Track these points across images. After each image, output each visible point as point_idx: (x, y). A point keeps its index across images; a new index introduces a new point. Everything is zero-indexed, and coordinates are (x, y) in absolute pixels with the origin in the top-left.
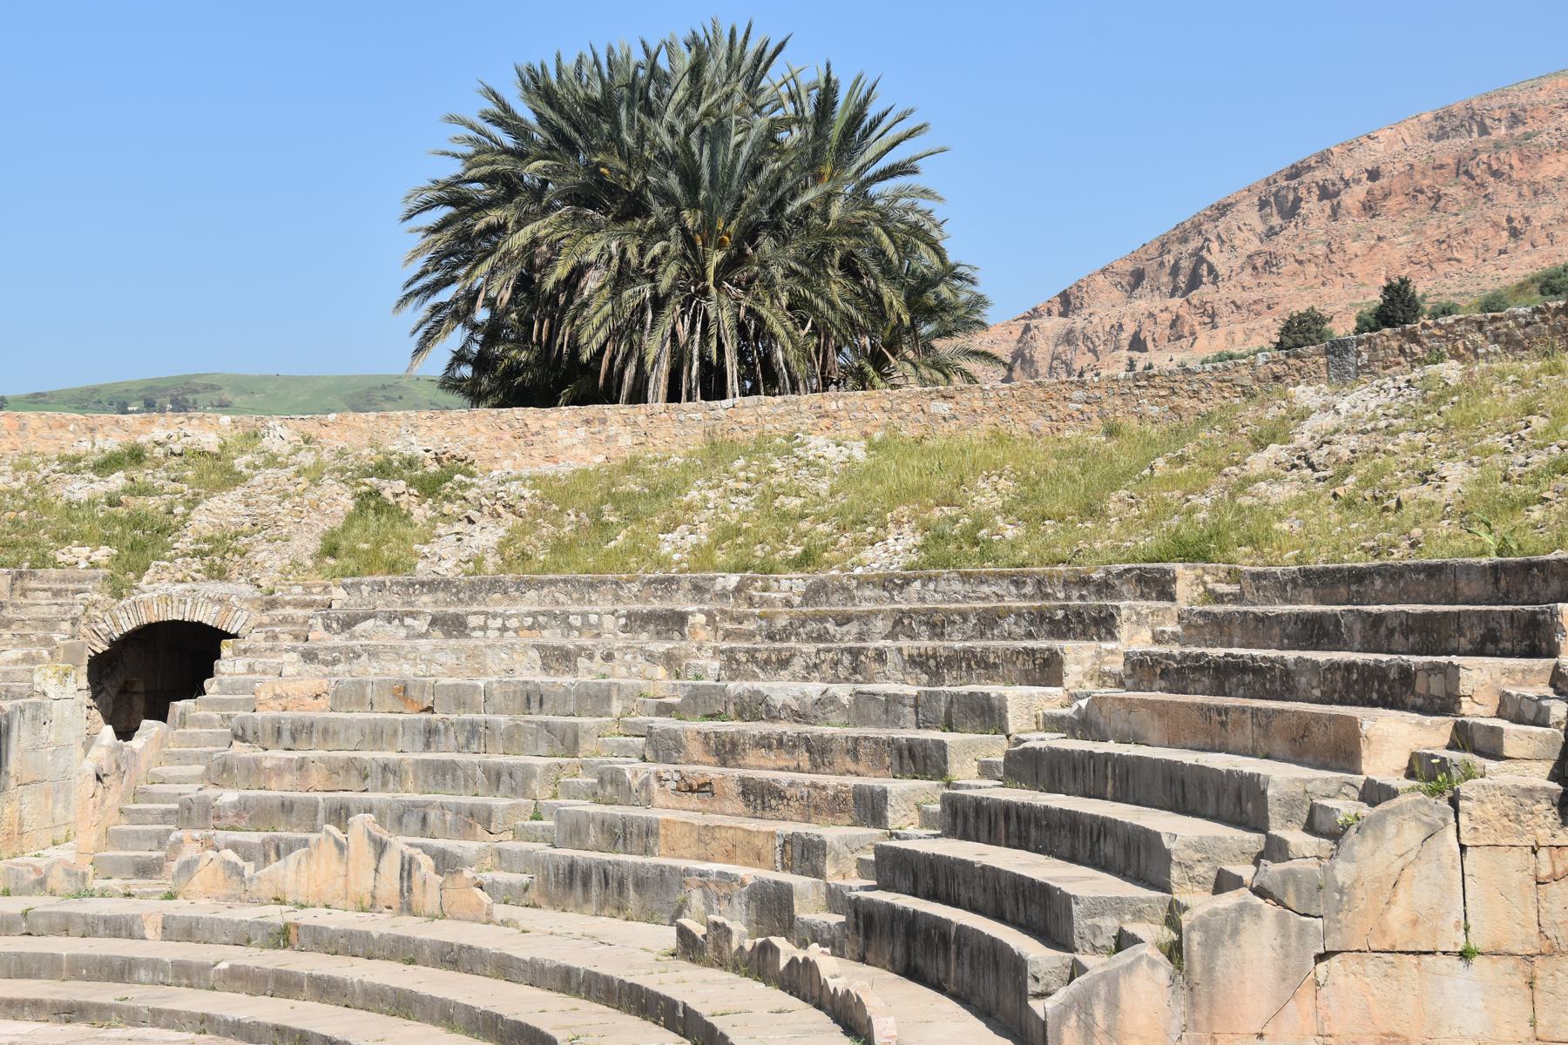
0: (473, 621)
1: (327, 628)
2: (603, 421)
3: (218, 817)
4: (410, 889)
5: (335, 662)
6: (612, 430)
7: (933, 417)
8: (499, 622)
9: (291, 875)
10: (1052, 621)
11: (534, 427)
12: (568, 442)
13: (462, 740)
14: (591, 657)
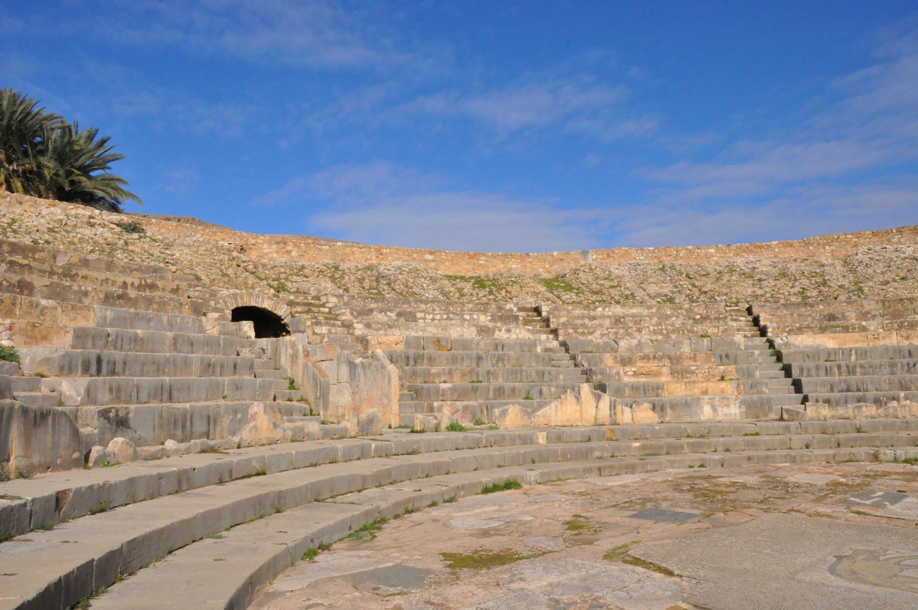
0: (419, 315)
1: (352, 314)
2: (286, 243)
4: (615, 414)
5: (380, 329)
6: (289, 248)
7: (426, 261)
8: (431, 316)
9: (553, 413)
10: (694, 319)
11: (253, 241)
13: (494, 362)
14: (500, 330)
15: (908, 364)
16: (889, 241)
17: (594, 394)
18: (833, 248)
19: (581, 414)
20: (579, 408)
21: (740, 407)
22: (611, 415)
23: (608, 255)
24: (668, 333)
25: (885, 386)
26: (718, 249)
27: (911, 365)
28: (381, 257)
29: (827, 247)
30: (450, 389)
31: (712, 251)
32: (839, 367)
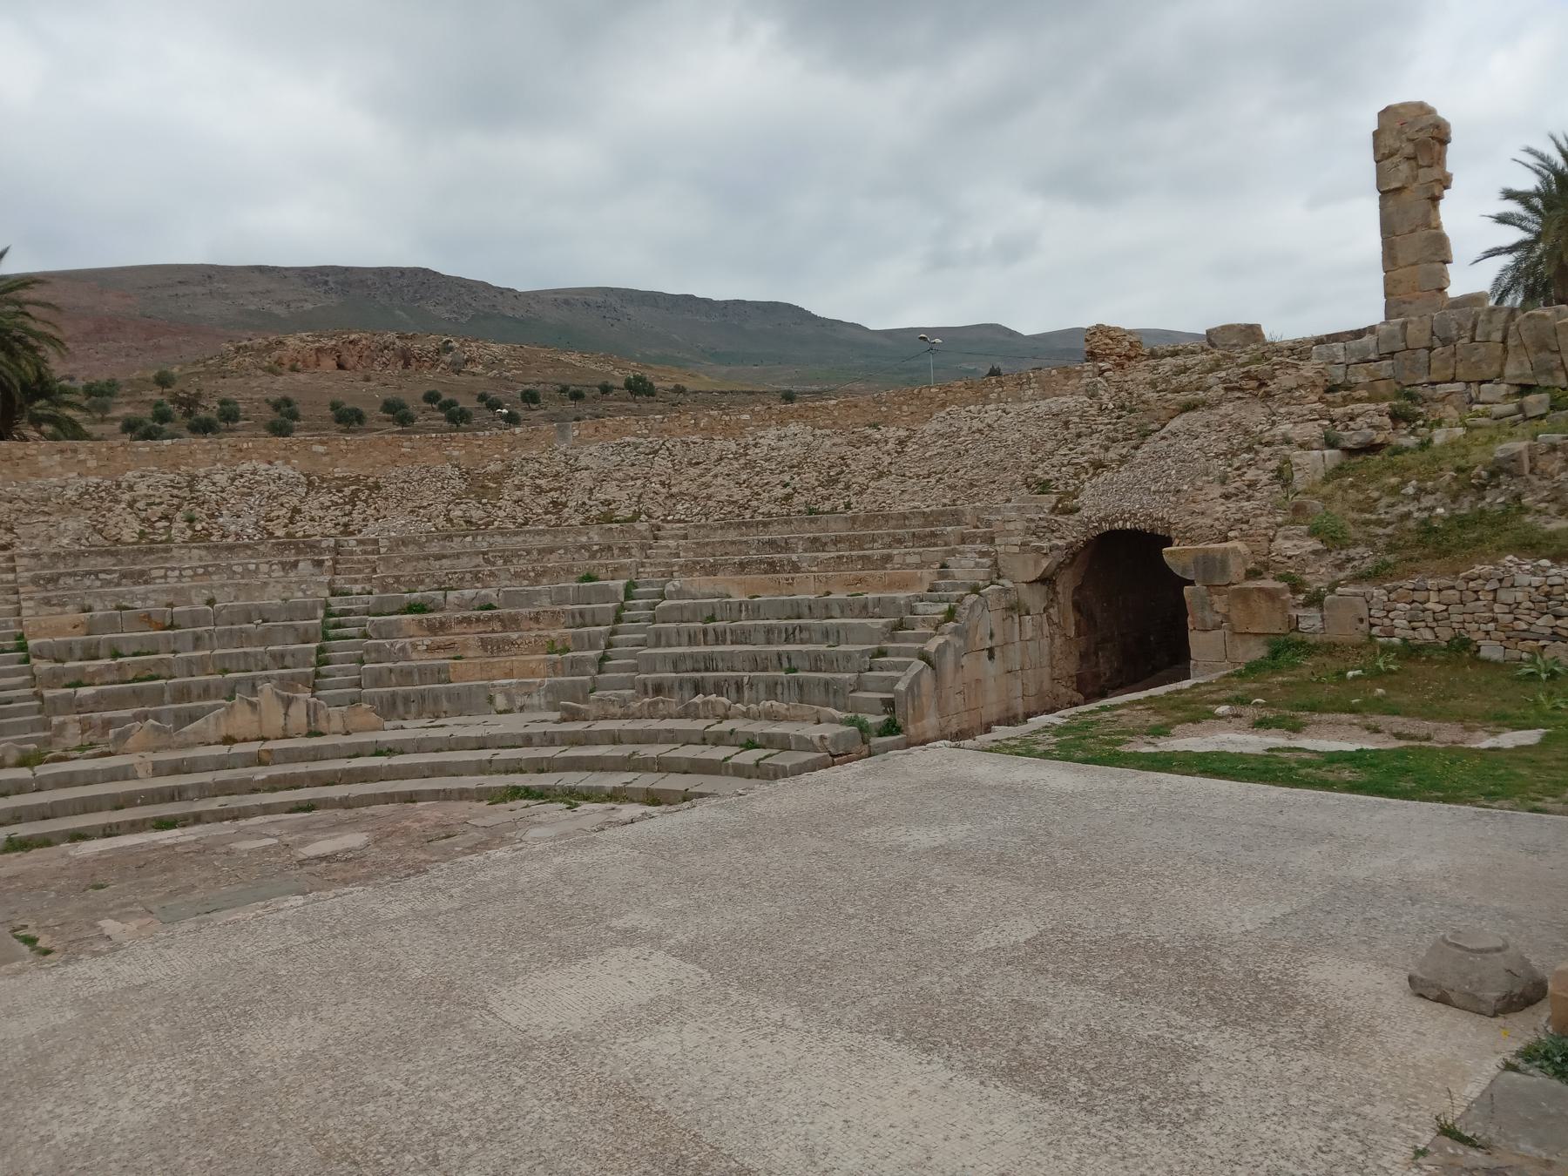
2: (75, 451)
3: (80, 706)
4: (316, 721)
6: (82, 457)
8: (177, 573)
11: (20, 453)
12: (47, 464)
16: (986, 396)
17: (281, 698)
18: (913, 409)
19: (260, 727)
20: (256, 718)
22: (309, 723)
23: (596, 430)
25: (738, 665)
28: (239, 455)
29: (905, 408)
30: (93, 696)
32: (705, 632)
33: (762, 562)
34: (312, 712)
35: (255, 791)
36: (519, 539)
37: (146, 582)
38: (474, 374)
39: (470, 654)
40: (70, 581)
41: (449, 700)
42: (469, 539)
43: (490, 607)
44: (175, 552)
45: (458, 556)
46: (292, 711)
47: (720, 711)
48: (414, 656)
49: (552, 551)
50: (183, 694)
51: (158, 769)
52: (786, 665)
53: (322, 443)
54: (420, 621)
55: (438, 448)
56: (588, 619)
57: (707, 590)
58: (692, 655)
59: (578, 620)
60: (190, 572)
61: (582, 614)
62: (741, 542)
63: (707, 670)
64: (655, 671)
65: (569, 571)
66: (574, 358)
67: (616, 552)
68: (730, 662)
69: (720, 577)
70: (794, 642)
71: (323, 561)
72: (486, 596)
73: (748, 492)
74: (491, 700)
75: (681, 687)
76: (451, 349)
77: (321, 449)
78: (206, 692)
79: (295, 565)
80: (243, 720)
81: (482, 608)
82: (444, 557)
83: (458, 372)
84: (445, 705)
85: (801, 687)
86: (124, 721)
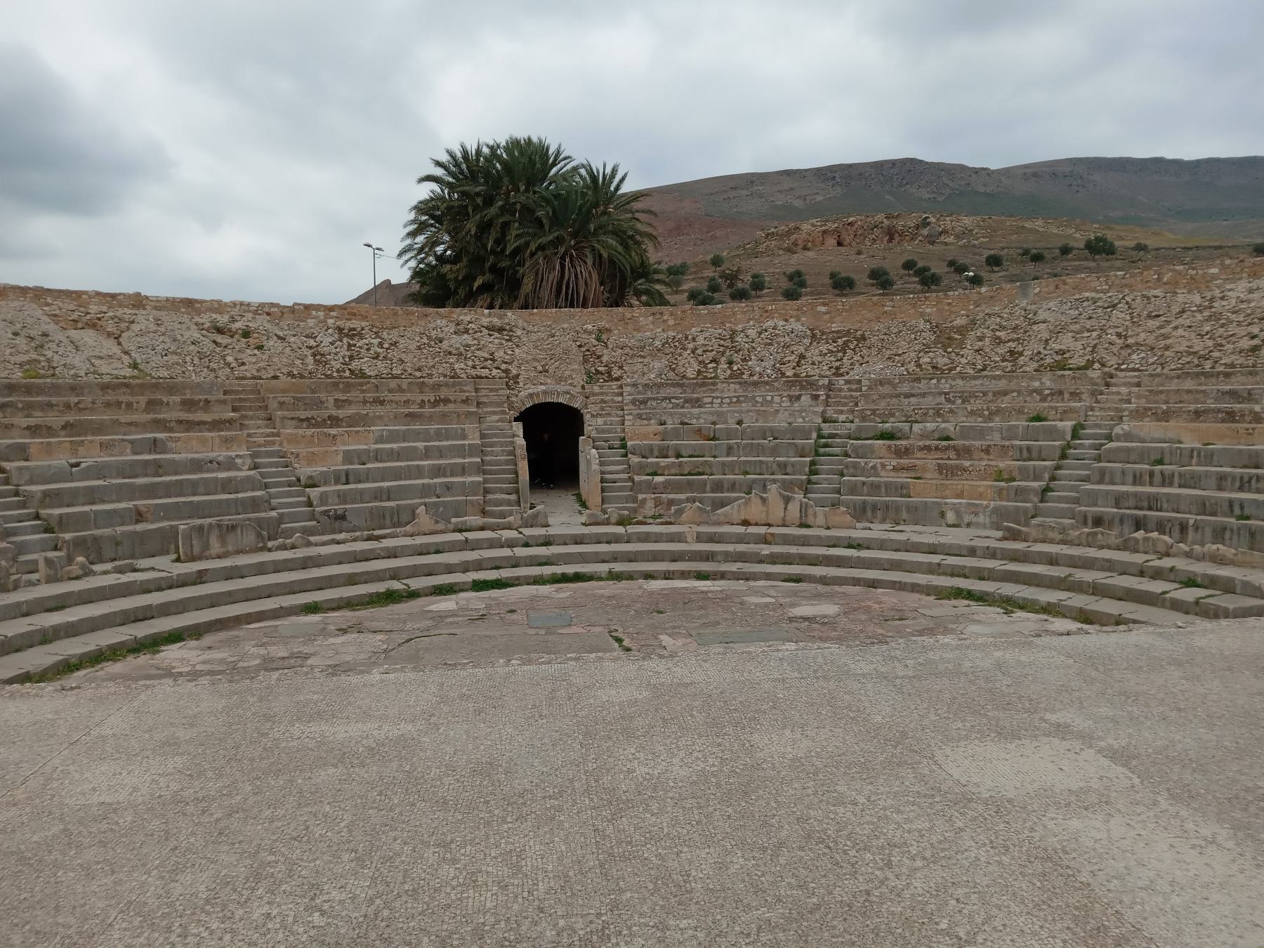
2: (661, 314)
4: (806, 516)
11: (629, 316)
15: (1242, 478)
21: (990, 516)
23: (1057, 287)
24: (990, 414)
26: (1223, 267)
27: (1246, 479)
30: (663, 483)
31: (1215, 271)
32: (1152, 474)
33: (1219, 411)
34: (804, 509)
35: (761, 562)
36: (978, 382)
37: (700, 406)
38: (946, 244)
39: (928, 475)
40: (654, 403)
41: (908, 511)
42: (934, 381)
43: (948, 438)
44: (719, 386)
45: (923, 395)
46: (790, 506)
47: (1162, 548)
48: (883, 473)
49: (1005, 393)
50: (718, 487)
51: (700, 538)
52: (1237, 511)
53: (824, 304)
54: (889, 446)
55: (914, 306)
56: (1034, 454)
57: (1157, 435)
58: (1135, 494)
59: (1025, 454)
60: (728, 400)
61: (1029, 449)
62: (1197, 392)
63: (1150, 509)
64: (1096, 505)
65: (1020, 411)
66: (1038, 224)
67: (1066, 396)
68: (1176, 504)
69: (1172, 423)
70: (1249, 491)
71: (818, 396)
72: (945, 429)
73: (1210, 343)
74: (943, 515)
75: (1121, 522)
76: (928, 224)
77: (823, 309)
78: (733, 487)
79: (798, 398)
80: (755, 510)
81: (940, 439)
82: (913, 395)
83: (933, 243)
84: (905, 515)
85: (1252, 534)
86: (680, 502)
